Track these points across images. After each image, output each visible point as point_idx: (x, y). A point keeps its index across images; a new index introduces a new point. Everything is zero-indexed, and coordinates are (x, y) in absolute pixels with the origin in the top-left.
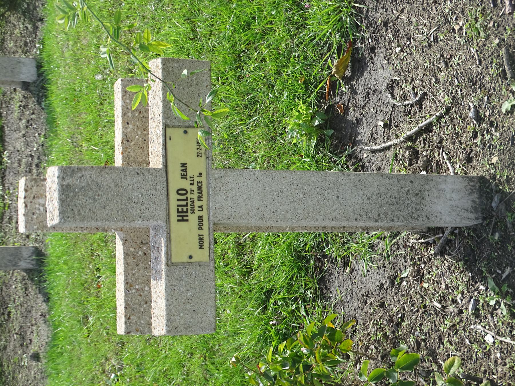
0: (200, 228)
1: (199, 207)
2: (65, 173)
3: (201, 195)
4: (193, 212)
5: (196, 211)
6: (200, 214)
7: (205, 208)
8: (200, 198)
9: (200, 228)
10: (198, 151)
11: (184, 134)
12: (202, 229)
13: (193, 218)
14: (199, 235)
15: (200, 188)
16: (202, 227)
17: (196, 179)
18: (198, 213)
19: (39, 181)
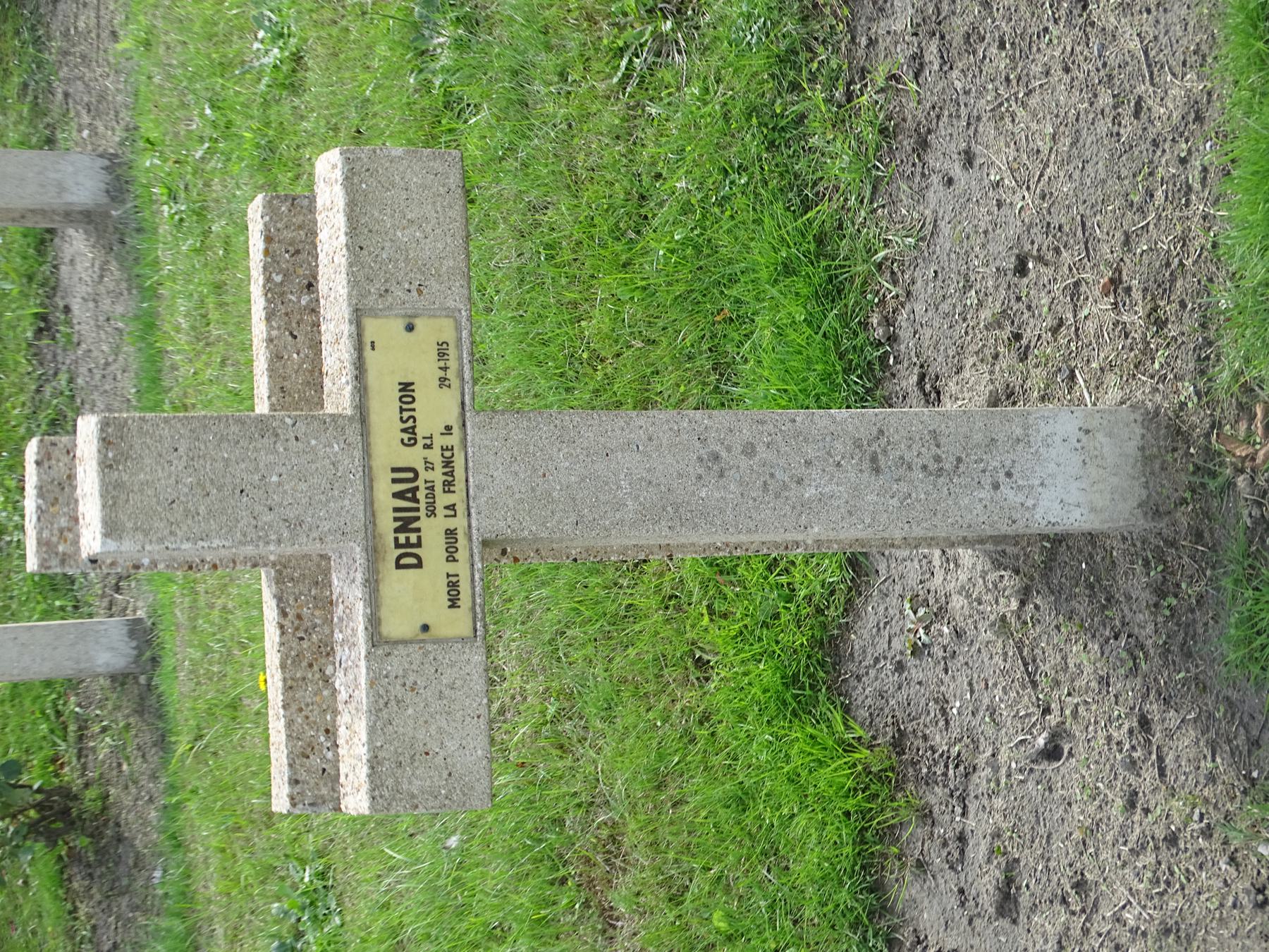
0: (451, 558)
1: (446, 508)
3: (450, 479)
6: (452, 523)
7: (461, 509)
8: (448, 486)
9: (451, 558)
10: (442, 374)
11: (405, 333)
12: (455, 560)
14: (448, 575)
15: (448, 463)
16: (457, 556)
17: (439, 441)
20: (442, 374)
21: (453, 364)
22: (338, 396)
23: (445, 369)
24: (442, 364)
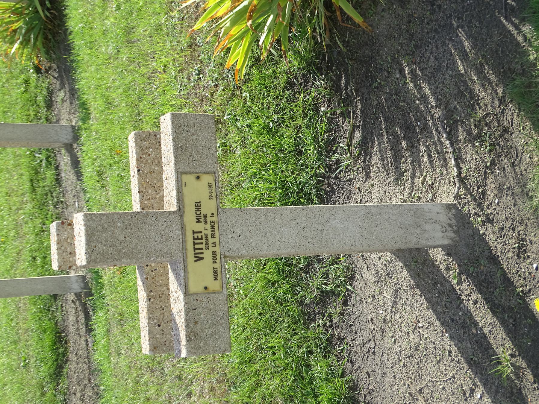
1: (213, 243)
2: (88, 218)
4: (207, 248)
5: (210, 247)
6: (215, 249)
7: (217, 243)
9: (214, 262)
10: (210, 194)
12: (216, 263)
13: (207, 255)
14: (214, 268)
17: (209, 219)
18: (211, 249)
19: (66, 225)
20: (210, 194)
21: (213, 191)
22: (170, 203)
23: (210, 193)
24: (210, 191)
